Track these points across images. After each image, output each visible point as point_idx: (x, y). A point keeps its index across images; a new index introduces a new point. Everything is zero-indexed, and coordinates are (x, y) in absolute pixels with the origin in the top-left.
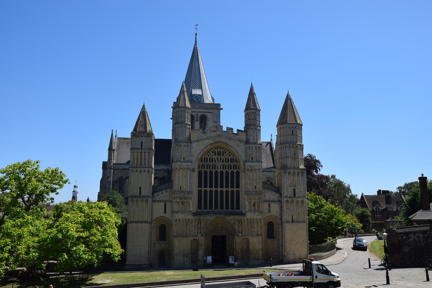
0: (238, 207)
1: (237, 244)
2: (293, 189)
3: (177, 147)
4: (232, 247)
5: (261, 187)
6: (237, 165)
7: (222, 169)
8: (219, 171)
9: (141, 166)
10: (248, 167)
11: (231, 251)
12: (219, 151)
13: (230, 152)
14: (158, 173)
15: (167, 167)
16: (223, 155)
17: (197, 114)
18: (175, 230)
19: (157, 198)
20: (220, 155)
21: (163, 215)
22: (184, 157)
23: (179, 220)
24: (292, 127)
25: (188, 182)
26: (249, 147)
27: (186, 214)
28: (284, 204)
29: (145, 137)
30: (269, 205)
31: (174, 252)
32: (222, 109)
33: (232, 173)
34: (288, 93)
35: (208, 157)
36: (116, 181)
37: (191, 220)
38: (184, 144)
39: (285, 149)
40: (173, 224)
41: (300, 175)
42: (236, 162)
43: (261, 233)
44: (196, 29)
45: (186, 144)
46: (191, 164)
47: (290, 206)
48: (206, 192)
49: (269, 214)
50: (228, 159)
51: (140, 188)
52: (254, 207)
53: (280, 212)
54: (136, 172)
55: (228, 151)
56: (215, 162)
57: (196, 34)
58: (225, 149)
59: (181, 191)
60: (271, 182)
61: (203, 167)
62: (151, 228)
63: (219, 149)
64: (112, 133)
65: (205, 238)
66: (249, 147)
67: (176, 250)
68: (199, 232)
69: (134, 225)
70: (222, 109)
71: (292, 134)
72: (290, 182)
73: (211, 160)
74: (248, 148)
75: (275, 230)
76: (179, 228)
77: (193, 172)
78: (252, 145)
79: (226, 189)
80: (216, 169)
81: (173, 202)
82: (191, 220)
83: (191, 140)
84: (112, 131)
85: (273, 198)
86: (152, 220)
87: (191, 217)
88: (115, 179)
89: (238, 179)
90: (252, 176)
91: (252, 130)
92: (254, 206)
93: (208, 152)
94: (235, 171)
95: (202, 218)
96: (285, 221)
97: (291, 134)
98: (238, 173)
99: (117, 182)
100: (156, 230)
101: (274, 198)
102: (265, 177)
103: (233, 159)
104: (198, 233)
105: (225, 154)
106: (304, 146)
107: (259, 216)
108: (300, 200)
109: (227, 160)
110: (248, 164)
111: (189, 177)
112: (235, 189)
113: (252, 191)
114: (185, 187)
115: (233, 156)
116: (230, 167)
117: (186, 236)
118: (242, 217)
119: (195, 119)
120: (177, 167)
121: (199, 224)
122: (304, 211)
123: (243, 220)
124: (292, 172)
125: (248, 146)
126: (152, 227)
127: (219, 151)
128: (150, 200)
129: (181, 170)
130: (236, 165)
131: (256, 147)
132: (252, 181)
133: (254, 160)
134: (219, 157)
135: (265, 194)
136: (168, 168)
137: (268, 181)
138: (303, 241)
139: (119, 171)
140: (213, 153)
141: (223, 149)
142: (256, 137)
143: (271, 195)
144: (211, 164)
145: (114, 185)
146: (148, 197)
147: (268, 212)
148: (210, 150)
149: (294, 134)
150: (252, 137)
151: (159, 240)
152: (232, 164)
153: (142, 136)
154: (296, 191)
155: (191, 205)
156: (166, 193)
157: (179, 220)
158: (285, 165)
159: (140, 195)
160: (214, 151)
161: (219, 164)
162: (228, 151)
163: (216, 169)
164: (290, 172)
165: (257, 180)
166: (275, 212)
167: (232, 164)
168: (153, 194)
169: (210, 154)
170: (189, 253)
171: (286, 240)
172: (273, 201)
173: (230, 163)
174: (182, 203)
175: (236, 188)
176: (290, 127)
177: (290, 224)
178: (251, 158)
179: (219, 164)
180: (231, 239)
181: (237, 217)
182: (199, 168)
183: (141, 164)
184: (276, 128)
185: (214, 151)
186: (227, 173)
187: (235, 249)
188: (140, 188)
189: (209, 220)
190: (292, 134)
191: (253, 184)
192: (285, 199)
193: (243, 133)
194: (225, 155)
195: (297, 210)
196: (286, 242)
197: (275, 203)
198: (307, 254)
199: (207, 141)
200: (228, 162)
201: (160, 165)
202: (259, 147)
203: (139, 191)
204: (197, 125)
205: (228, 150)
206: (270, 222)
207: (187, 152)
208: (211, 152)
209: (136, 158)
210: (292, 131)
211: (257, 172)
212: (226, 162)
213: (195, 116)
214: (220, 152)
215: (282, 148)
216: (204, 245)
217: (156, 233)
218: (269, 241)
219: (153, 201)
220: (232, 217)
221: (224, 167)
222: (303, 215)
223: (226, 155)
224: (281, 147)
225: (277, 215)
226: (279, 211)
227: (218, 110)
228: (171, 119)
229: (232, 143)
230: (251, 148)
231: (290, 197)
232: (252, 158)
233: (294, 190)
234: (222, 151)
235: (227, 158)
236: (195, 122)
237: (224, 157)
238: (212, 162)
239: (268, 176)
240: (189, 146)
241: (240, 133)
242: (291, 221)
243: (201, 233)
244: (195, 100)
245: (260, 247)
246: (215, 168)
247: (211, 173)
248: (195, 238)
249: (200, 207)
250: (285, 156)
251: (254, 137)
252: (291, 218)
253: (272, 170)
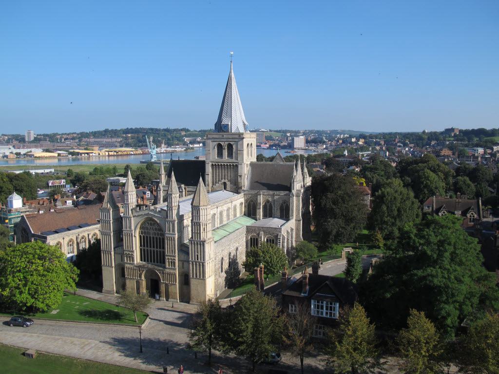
8: (152, 236)
30: (183, 264)
33: (160, 239)
49: (183, 270)
60: (287, 204)
73: (147, 228)
94: (161, 237)
98: (163, 240)
109: (156, 229)
112: (162, 250)
116: (158, 234)
137: (285, 203)
152: (160, 232)
161: (151, 232)
174: (130, 257)
179: (151, 232)
186: (157, 238)
204: (225, 153)
233: (198, 255)
241: (163, 211)
249: (141, 260)
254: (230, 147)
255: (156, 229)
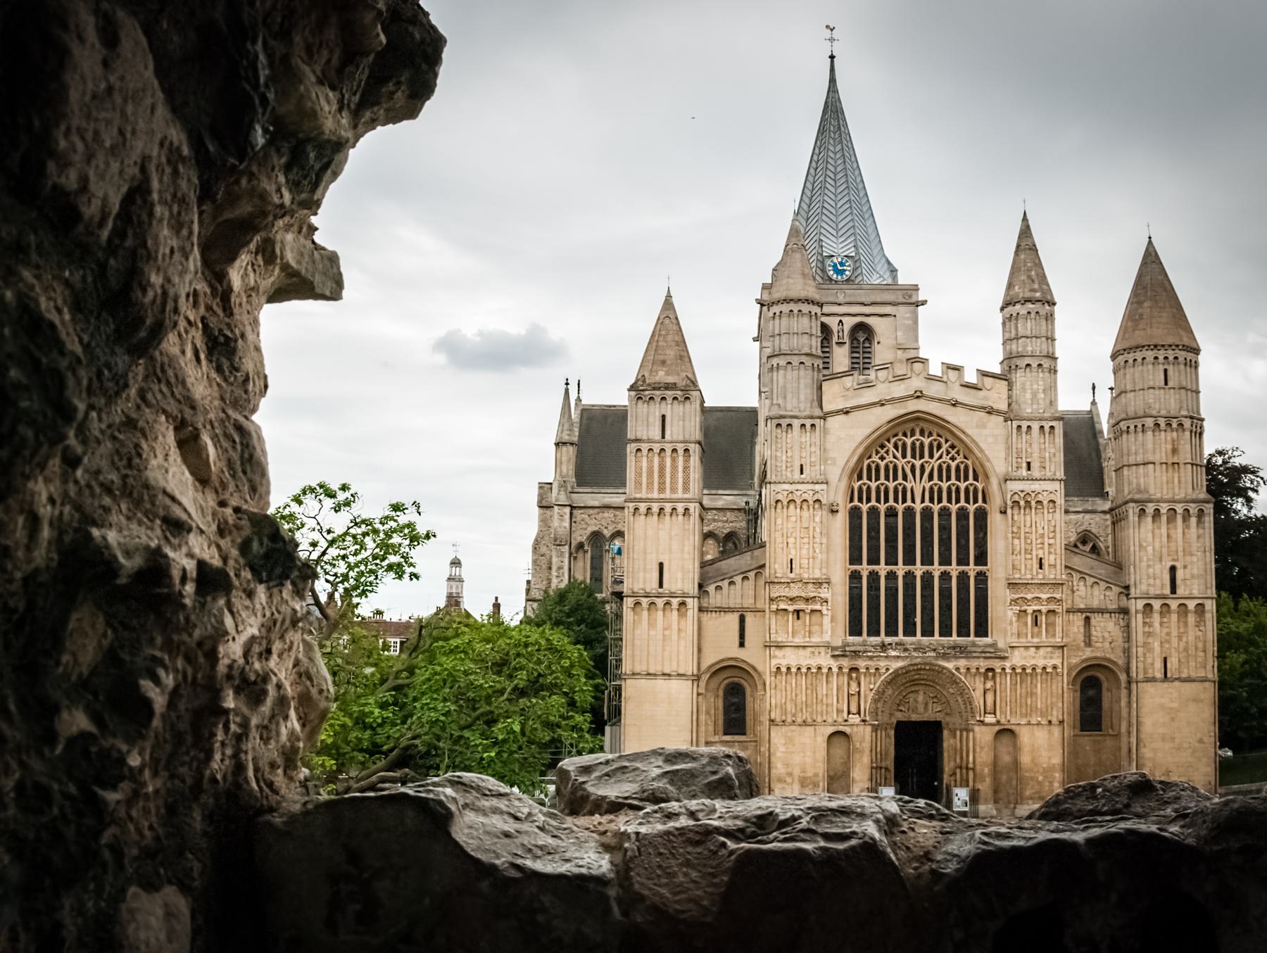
0: (982, 630)
1: (978, 749)
2: (1168, 567)
3: (779, 431)
4: (961, 758)
5: (1058, 561)
6: (980, 486)
7: (927, 503)
8: (918, 507)
9: (662, 496)
10: (1016, 496)
11: (958, 771)
12: (918, 444)
13: (956, 443)
14: (714, 520)
15: (745, 499)
16: (931, 456)
17: (841, 321)
18: (773, 701)
19: (715, 598)
20: (922, 457)
21: (735, 652)
22: (802, 466)
23: (789, 669)
24: (1166, 358)
25: (816, 545)
26: (1019, 427)
27: (810, 649)
28: (1137, 621)
29: (675, 402)
30: (1087, 619)
31: (773, 771)
32: (924, 303)
33: (962, 514)
34: (1150, 242)
35: (879, 461)
36: (581, 546)
37: (825, 670)
38: (803, 421)
39: (1140, 434)
40: (768, 683)
41: (1193, 520)
42: (976, 479)
43: (1061, 717)
44: (832, 40)
45: (808, 423)
46: (824, 486)
47: (1157, 625)
48: (874, 577)
49: (1088, 653)
50: (949, 468)
51: (661, 565)
52: (1036, 629)
53: (1122, 644)
54: (646, 515)
55: (949, 444)
56: (905, 478)
57: (832, 57)
58: (939, 435)
59: (792, 576)
61: (863, 495)
62: (698, 694)
63: (917, 436)
64: (567, 391)
65: (875, 729)
66: (1019, 427)
67: (779, 765)
68: (854, 709)
69: (643, 683)
70: (924, 303)
71: (1166, 383)
72: (1157, 545)
74: (1015, 431)
75: (1106, 704)
76: (789, 697)
77: (830, 515)
78: (1029, 423)
79: (943, 568)
80: (909, 503)
81: (767, 611)
82: (825, 670)
83: (827, 407)
84: (567, 384)
85: (1100, 600)
86: (699, 669)
87: (825, 661)
88: (579, 539)
89: (981, 535)
90: (1028, 524)
91: (1028, 369)
92: (1036, 625)
93: (882, 446)
94: (972, 508)
95: (861, 664)
96: (1141, 676)
97: (1163, 383)
98: (982, 516)
99: (586, 548)
100: (712, 700)
101: (1102, 597)
102: (1073, 530)
103: (966, 468)
104: (849, 713)
105: (938, 451)
106: (1205, 423)
107: (1051, 658)
108: (1191, 605)
109: (944, 473)
110: (1014, 486)
111: (818, 530)
112: (972, 570)
113: (1029, 576)
114: (806, 561)
115: (965, 458)
116: (954, 494)
117: (814, 723)
118: (997, 665)
119: (835, 339)
120: (780, 497)
121: (854, 686)
122: (1205, 641)
123: (998, 670)
124: (1165, 511)
125: (1015, 424)
126: (700, 691)
127: (918, 444)
128: (692, 603)
129: (792, 506)
130: (976, 490)
131: (1042, 427)
132: (1029, 541)
133: (1036, 473)
134: (918, 463)
135: (1075, 583)
136: (747, 503)
138: (1201, 741)
139: (591, 511)
140: (898, 451)
141: (930, 434)
142: (1042, 395)
143: (1092, 586)
144: (891, 485)
145: (575, 558)
146: (685, 595)
147: (1082, 644)
148: (889, 441)
149: (1171, 384)
150: (1028, 396)
151: (725, 734)
152: (963, 486)
153: (663, 399)
154: (1180, 574)
155: (826, 620)
156: (746, 582)
157: (789, 669)
158: (1142, 487)
159: (660, 590)
160: (900, 444)
161: (918, 486)
162: (949, 444)
163: (909, 503)
164: (1157, 510)
165: (1046, 539)
166: (1107, 645)
167: (963, 486)
168: (700, 586)
169: (887, 452)
170: (821, 775)
171: (1142, 736)
172: (1101, 611)
173: (953, 480)
175: (976, 565)
176: (1156, 358)
177: (1158, 684)
178: (1024, 465)
179: (918, 486)
180: (958, 733)
181: (983, 664)
182: (852, 500)
183: (662, 490)
184: (1110, 365)
185: (900, 444)
186: (945, 513)
187: (971, 765)
188: (661, 565)
189: (887, 669)
190: (1166, 383)
191: (1034, 553)
192: (1140, 604)
193: (997, 381)
194: (936, 455)
195: (1180, 638)
196: (1142, 745)
197: (1108, 615)
198: (1213, 783)
199: (879, 410)
200: (949, 479)
201: (720, 492)
202: (1052, 427)
203: (656, 575)
204: (841, 357)
205: (949, 438)
206: (1087, 678)
207: (813, 449)
208: (891, 446)
209: (644, 469)
210: (1166, 371)
211: (1046, 511)
212: (940, 479)
213: (835, 328)
214: (922, 445)
215: (1132, 427)
216: (871, 751)
217: (713, 712)
218: (1087, 741)
219: (701, 610)
220: (962, 663)
221: (934, 494)
222: (1202, 654)
223: (941, 457)
224: (1128, 427)
225: (1112, 657)
226: (1121, 640)
227: (912, 308)
228: (755, 340)
229: (956, 417)
230: (1024, 429)
231: (1157, 597)
232: (1029, 464)
233: (1173, 569)
234: (927, 441)
235: (944, 466)
236: (835, 347)
237: (935, 463)
238: (895, 479)
239: (1083, 528)
240: (818, 428)
242: (1159, 675)
243: (859, 713)
244: (835, 276)
245: (1057, 760)
246: (904, 501)
247: (891, 513)
248: (841, 728)
249: (855, 629)
250: (1140, 459)
251: (1034, 394)
252: (1159, 665)
253: (1095, 508)
254: (862, 335)
255: (944, 473)
